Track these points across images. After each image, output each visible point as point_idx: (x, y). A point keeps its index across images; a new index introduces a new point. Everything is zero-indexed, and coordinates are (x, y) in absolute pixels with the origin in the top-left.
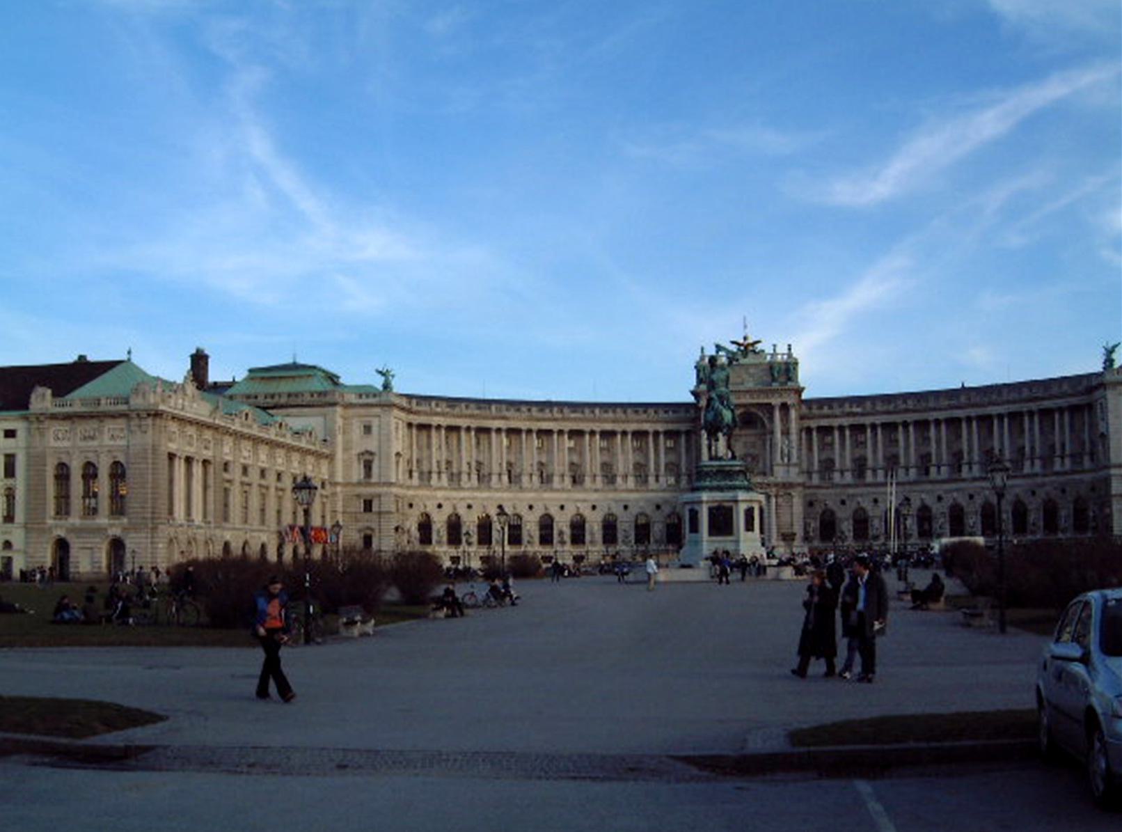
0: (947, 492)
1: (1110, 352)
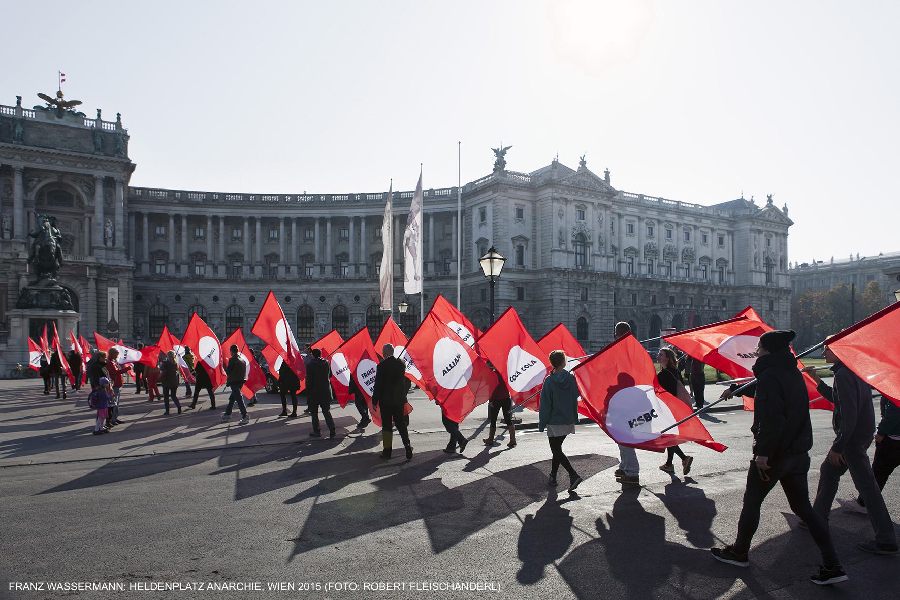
0: (294, 292)
1: (500, 154)
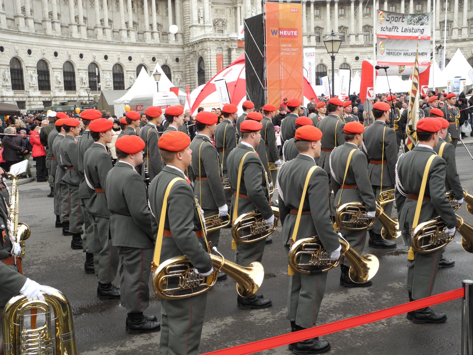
0: (361, 53)
